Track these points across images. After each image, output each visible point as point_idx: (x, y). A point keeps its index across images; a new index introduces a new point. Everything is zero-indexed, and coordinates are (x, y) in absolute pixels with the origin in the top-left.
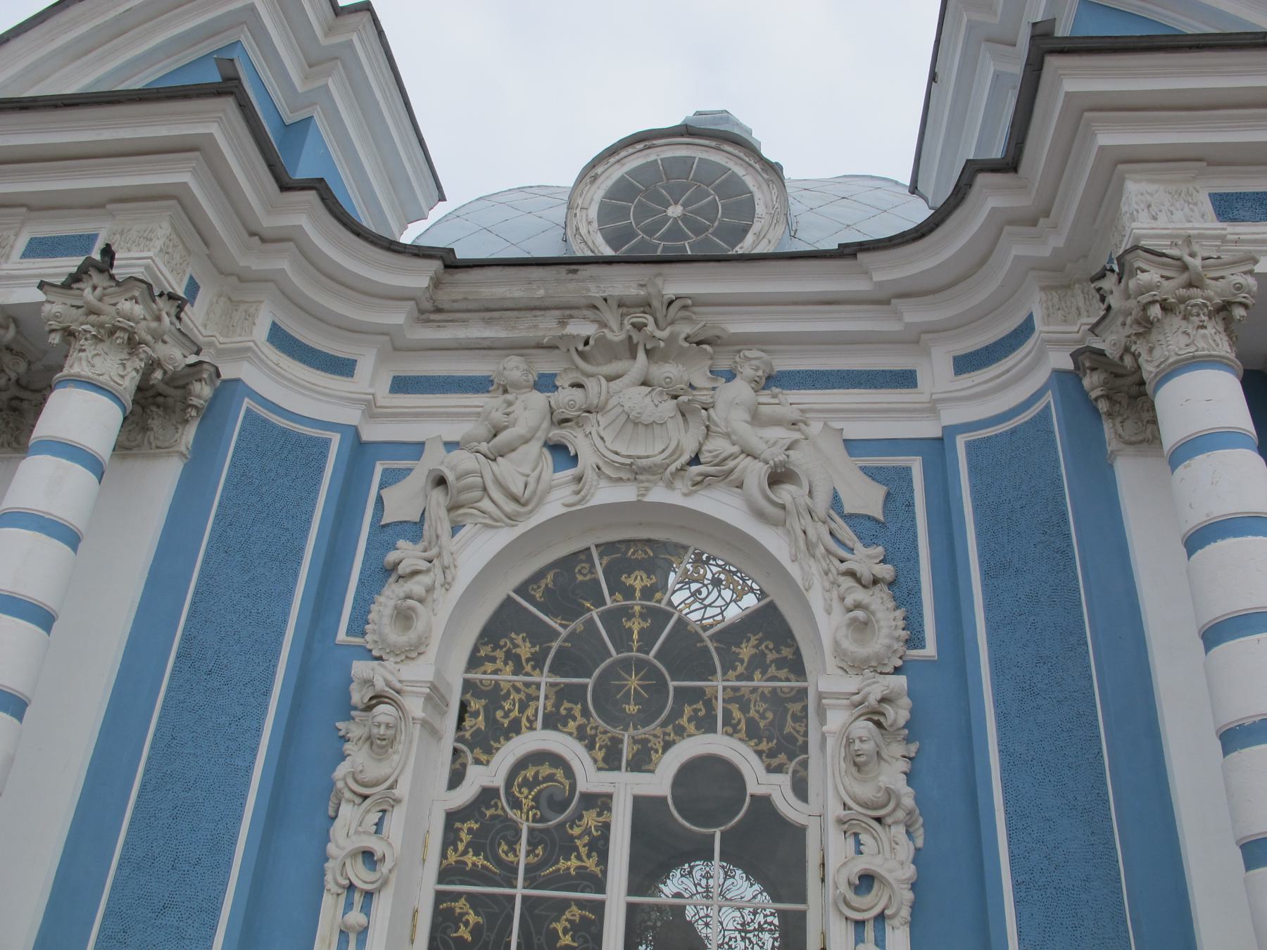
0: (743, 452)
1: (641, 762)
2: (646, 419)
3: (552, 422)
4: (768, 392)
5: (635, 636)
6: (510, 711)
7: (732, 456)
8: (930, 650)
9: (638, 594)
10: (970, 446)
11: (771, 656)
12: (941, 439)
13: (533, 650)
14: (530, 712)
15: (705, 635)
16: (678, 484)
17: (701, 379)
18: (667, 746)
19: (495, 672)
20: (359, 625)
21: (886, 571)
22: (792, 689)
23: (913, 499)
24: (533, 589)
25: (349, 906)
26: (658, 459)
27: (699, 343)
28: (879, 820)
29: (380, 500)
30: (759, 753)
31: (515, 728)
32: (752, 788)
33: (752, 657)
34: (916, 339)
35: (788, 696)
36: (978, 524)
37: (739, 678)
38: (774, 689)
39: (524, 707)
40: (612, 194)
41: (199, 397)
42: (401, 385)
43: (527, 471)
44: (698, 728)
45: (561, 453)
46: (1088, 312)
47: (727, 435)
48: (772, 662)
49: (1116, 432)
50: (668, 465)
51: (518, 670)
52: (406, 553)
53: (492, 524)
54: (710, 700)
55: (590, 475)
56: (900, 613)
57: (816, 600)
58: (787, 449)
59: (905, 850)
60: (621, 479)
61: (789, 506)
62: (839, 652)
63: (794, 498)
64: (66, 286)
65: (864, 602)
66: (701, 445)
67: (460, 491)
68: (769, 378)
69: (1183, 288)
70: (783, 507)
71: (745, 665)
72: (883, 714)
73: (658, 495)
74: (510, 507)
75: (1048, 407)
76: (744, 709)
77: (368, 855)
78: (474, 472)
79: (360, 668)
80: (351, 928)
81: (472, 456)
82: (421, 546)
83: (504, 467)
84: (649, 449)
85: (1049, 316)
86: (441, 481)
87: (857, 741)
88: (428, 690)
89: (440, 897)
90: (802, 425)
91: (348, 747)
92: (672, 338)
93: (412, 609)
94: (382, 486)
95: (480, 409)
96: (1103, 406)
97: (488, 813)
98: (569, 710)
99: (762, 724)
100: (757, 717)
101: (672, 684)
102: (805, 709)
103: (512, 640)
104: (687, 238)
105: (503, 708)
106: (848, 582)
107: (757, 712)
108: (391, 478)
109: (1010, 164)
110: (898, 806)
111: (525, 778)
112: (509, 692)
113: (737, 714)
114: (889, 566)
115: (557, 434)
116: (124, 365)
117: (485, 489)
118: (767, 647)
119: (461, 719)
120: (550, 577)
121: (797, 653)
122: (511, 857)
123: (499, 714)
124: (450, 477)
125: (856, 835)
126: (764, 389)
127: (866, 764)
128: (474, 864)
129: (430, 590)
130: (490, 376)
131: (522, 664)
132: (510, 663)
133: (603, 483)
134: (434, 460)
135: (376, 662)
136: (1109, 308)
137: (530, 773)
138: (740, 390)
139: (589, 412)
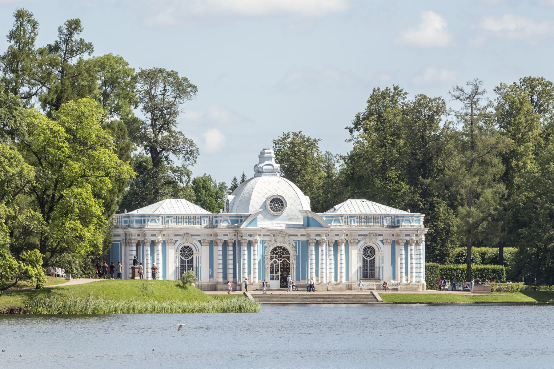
1: (281, 260)
108: (264, 243)
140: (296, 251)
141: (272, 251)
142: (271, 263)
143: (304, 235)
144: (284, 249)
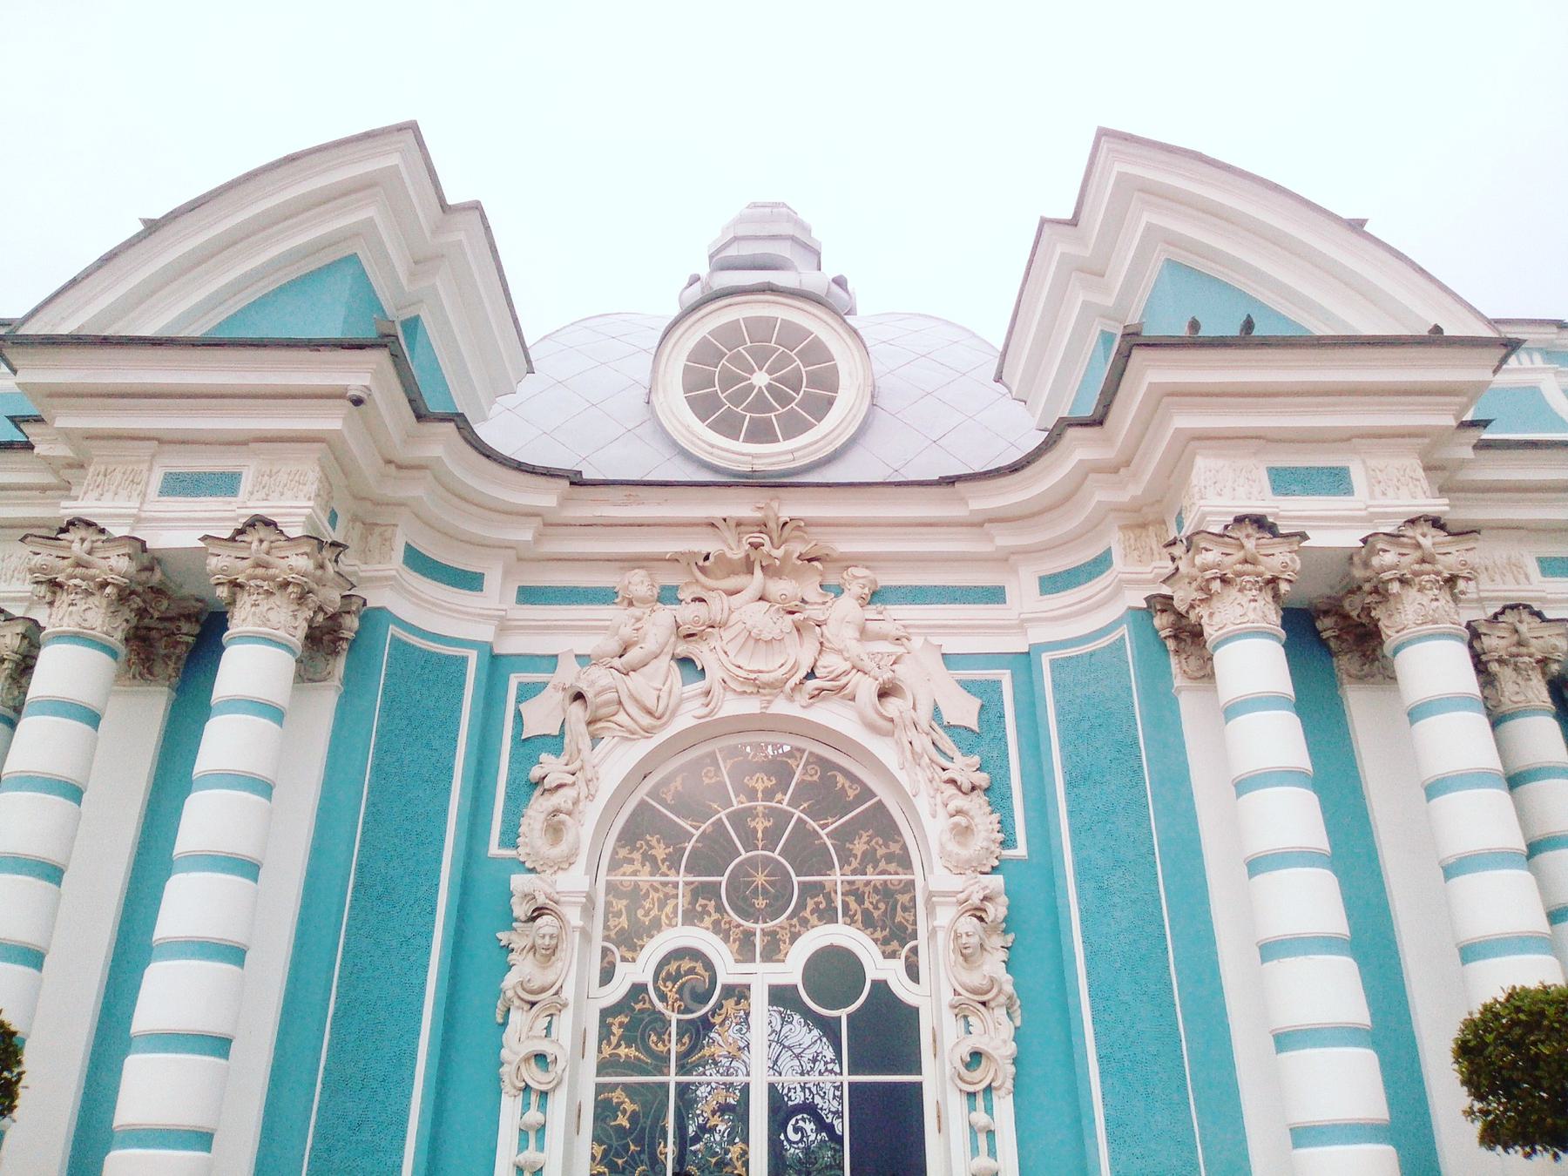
0: (854, 667)
1: (773, 951)
2: (766, 636)
3: (678, 636)
4: (874, 607)
5: (760, 835)
6: (650, 910)
7: (846, 673)
8: (1021, 850)
9: (760, 795)
10: (1053, 662)
11: (881, 852)
12: (1028, 653)
13: (667, 851)
14: (669, 909)
15: (823, 833)
16: (797, 696)
17: (812, 592)
18: (794, 937)
19: (635, 873)
20: (511, 837)
21: (982, 779)
22: (901, 881)
23: (1003, 709)
24: (663, 793)
25: (526, 1106)
26: (779, 674)
27: (810, 560)
28: (984, 1004)
29: (518, 715)
30: (876, 940)
31: (656, 925)
32: (871, 975)
33: (865, 853)
34: (1004, 559)
35: (898, 888)
36: (1061, 736)
37: (854, 872)
38: (885, 882)
39: (662, 905)
40: (695, 356)
41: (350, 630)
42: (528, 595)
43: (660, 686)
44: (820, 919)
46: (1160, 554)
47: (840, 652)
48: (882, 857)
49: (1181, 668)
50: (788, 679)
51: (655, 870)
52: (550, 767)
53: (630, 735)
54: (830, 893)
55: (717, 690)
56: (996, 817)
57: (923, 804)
58: (894, 663)
59: (1007, 1030)
60: (745, 692)
61: (896, 720)
62: (944, 853)
63: (901, 712)
64: (232, 539)
65: (964, 809)
66: (816, 661)
67: (598, 707)
68: (874, 594)
69: (1240, 563)
70: (892, 720)
71: (858, 860)
72: (985, 911)
73: (781, 707)
74: (646, 721)
75: (1122, 638)
76: (860, 901)
77: (540, 1058)
78: (610, 688)
79: (519, 882)
80: (531, 1127)
81: (607, 671)
82: (563, 759)
83: (636, 681)
84: (770, 665)
85: (1126, 556)
86: (579, 696)
87: (964, 936)
88: (584, 900)
89: (600, 1088)
90: (904, 640)
91: (512, 957)
92: (787, 555)
93: (562, 823)
94: (519, 701)
95: (608, 623)
96: (1171, 644)
97: (638, 1007)
98: (704, 906)
99: (876, 914)
100: (871, 907)
101: (795, 879)
102: (913, 899)
103: (647, 843)
104: (773, 409)
105: (644, 908)
106: (951, 790)
107: (871, 903)
108: (528, 692)
109: (1098, 421)
110: (1000, 991)
111: (669, 974)
112: (648, 891)
113: (853, 906)
114: (985, 775)
115: (683, 649)
116: (295, 617)
117: (620, 703)
118: (877, 843)
119: (606, 920)
120: (679, 779)
121: (905, 848)
122: (660, 1047)
123: (640, 913)
124: (589, 695)
125: (965, 1017)
126: (869, 604)
127: (972, 955)
128: (627, 1056)
129: (576, 803)
130: (614, 588)
131: (657, 863)
132: (647, 863)
133: (730, 695)
134: (568, 674)
135: (533, 876)
136: (1177, 569)
137: (673, 967)
138: (847, 607)
139: (713, 627)
140: (995, 794)
142: (616, 991)
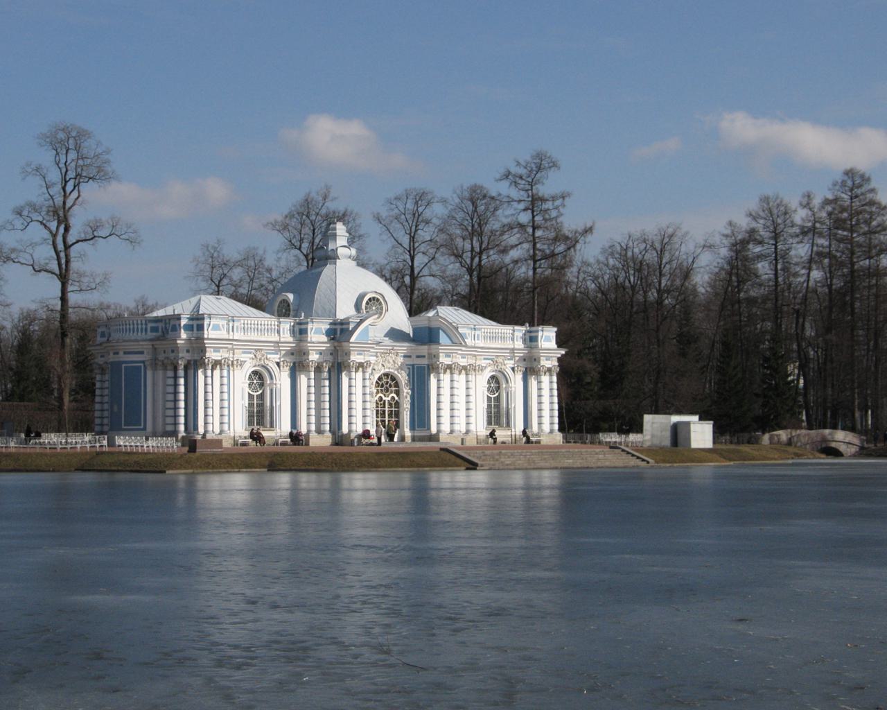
45: (383, 366)
84: (389, 365)
141: (377, 382)
143: (424, 357)
144: (393, 379)
